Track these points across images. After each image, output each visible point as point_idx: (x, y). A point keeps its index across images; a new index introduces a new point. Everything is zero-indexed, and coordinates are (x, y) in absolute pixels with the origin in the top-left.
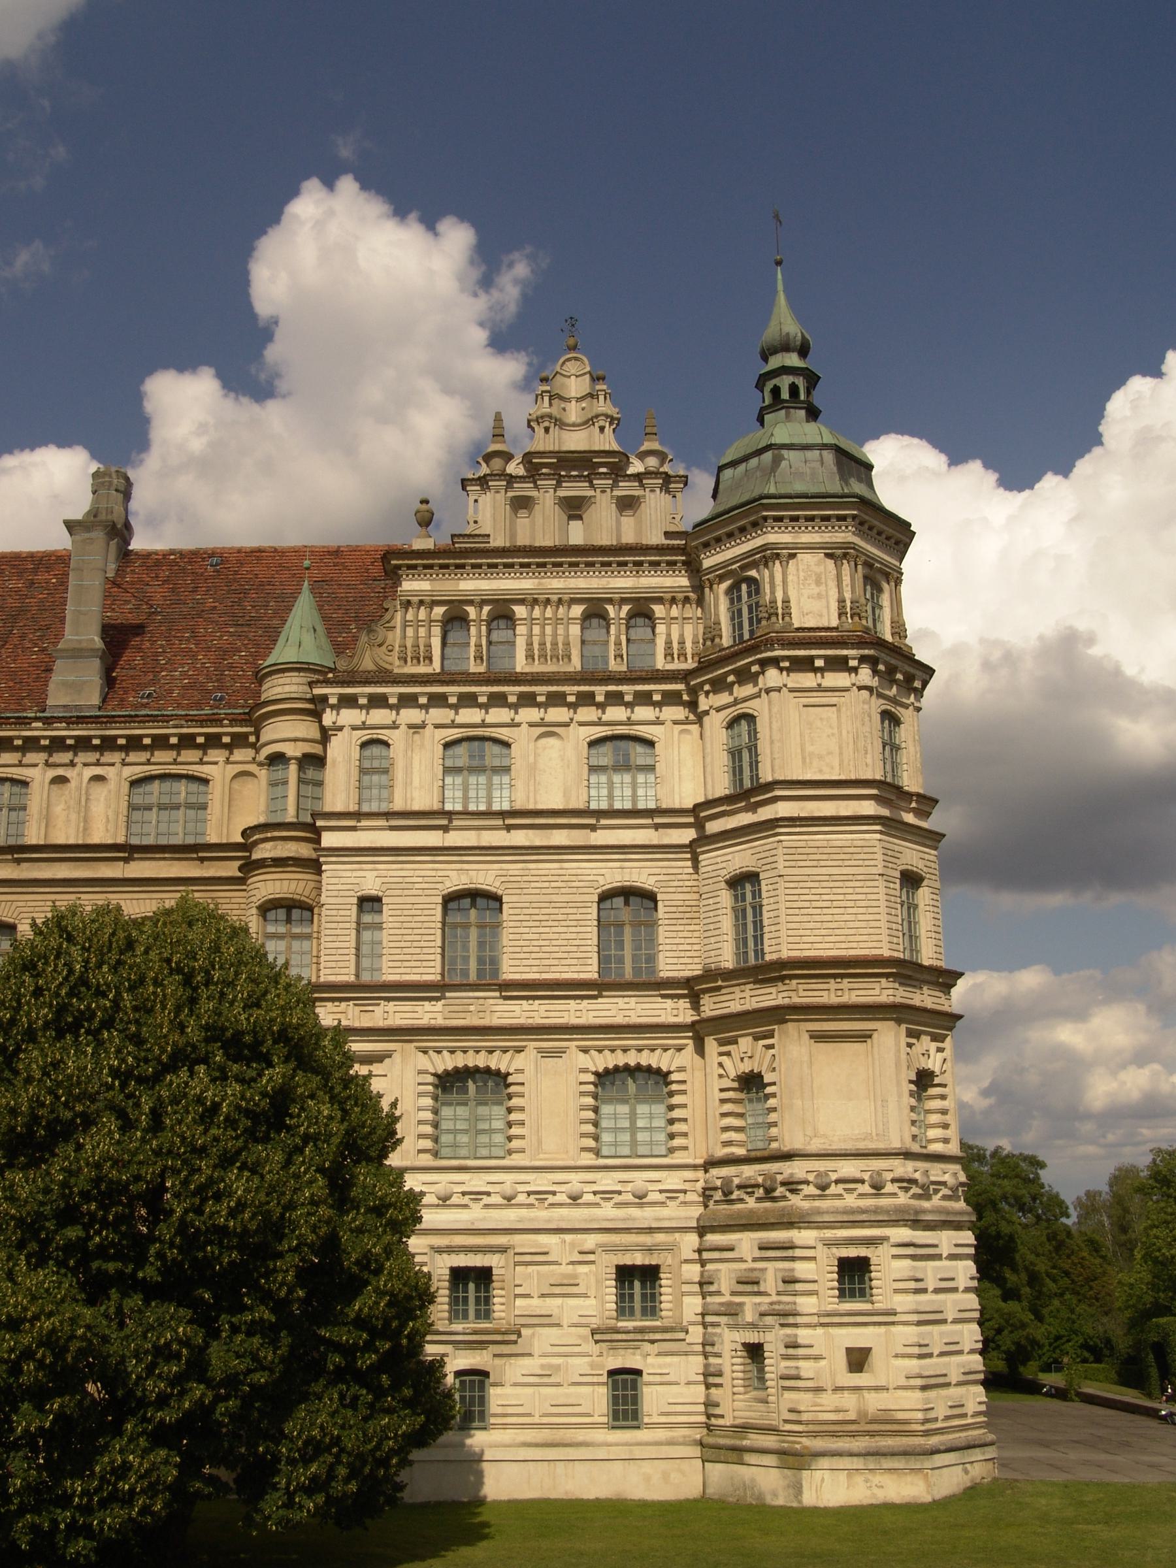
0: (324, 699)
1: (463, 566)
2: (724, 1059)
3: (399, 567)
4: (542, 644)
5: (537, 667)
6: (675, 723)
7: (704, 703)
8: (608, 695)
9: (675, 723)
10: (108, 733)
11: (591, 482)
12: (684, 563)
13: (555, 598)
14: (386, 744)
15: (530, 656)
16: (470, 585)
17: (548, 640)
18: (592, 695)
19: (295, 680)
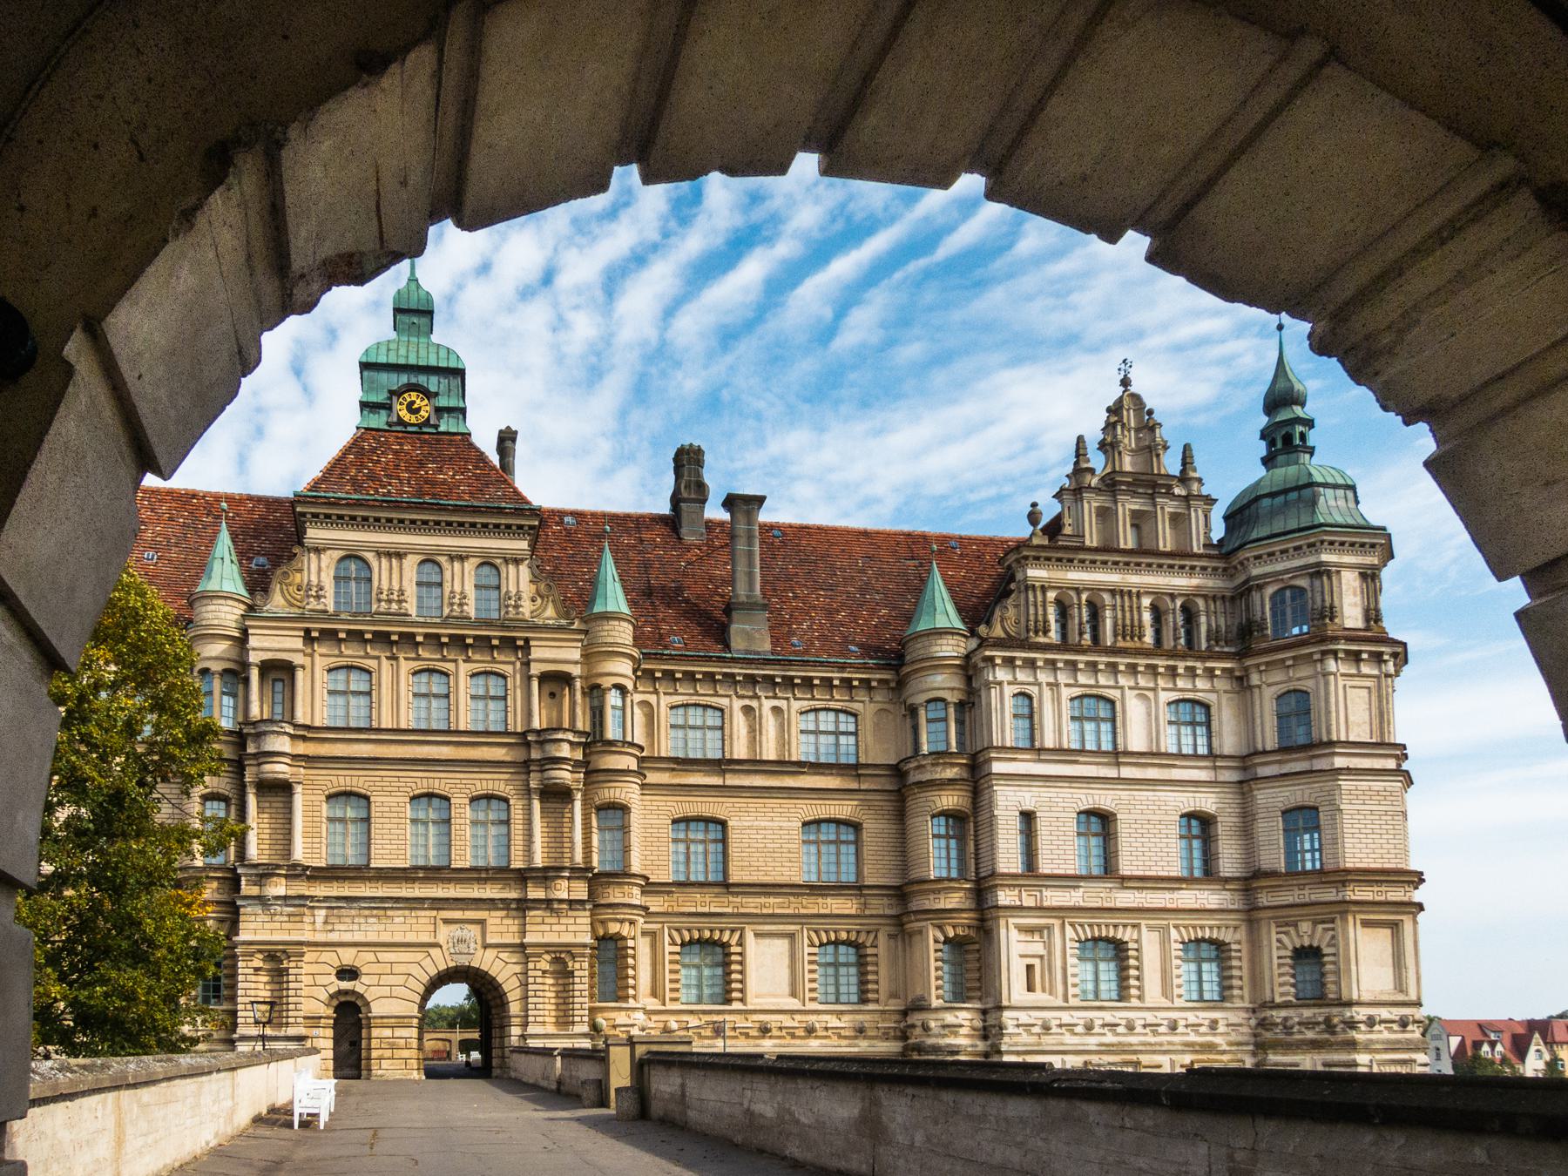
0: (991, 659)
1: (1071, 561)
2: (1282, 936)
3: (1026, 558)
4: (1124, 626)
5: (1121, 644)
6: (1225, 692)
7: (1255, 679)
8: (1187, 668)
9: (1225, 692)
10: (845, 675)
11: (1153, 499)
12: (1225, 570)
13: (1134, 590)
14: (1030, 697)
15: (1115, 635)
16: (1075, 576)
17: (1128, 622)
18: (1174, 668)
19: (951, 642)
